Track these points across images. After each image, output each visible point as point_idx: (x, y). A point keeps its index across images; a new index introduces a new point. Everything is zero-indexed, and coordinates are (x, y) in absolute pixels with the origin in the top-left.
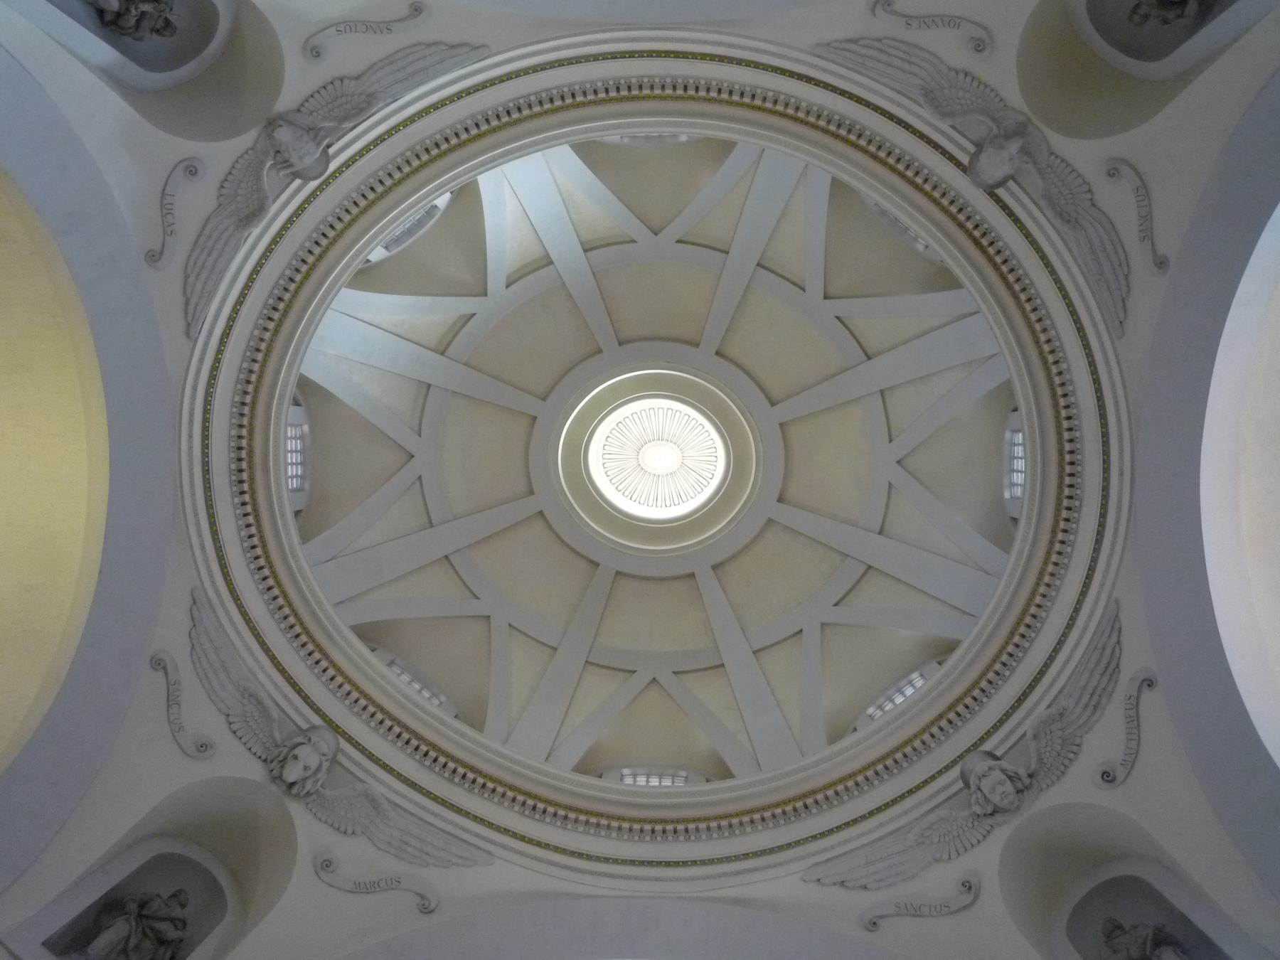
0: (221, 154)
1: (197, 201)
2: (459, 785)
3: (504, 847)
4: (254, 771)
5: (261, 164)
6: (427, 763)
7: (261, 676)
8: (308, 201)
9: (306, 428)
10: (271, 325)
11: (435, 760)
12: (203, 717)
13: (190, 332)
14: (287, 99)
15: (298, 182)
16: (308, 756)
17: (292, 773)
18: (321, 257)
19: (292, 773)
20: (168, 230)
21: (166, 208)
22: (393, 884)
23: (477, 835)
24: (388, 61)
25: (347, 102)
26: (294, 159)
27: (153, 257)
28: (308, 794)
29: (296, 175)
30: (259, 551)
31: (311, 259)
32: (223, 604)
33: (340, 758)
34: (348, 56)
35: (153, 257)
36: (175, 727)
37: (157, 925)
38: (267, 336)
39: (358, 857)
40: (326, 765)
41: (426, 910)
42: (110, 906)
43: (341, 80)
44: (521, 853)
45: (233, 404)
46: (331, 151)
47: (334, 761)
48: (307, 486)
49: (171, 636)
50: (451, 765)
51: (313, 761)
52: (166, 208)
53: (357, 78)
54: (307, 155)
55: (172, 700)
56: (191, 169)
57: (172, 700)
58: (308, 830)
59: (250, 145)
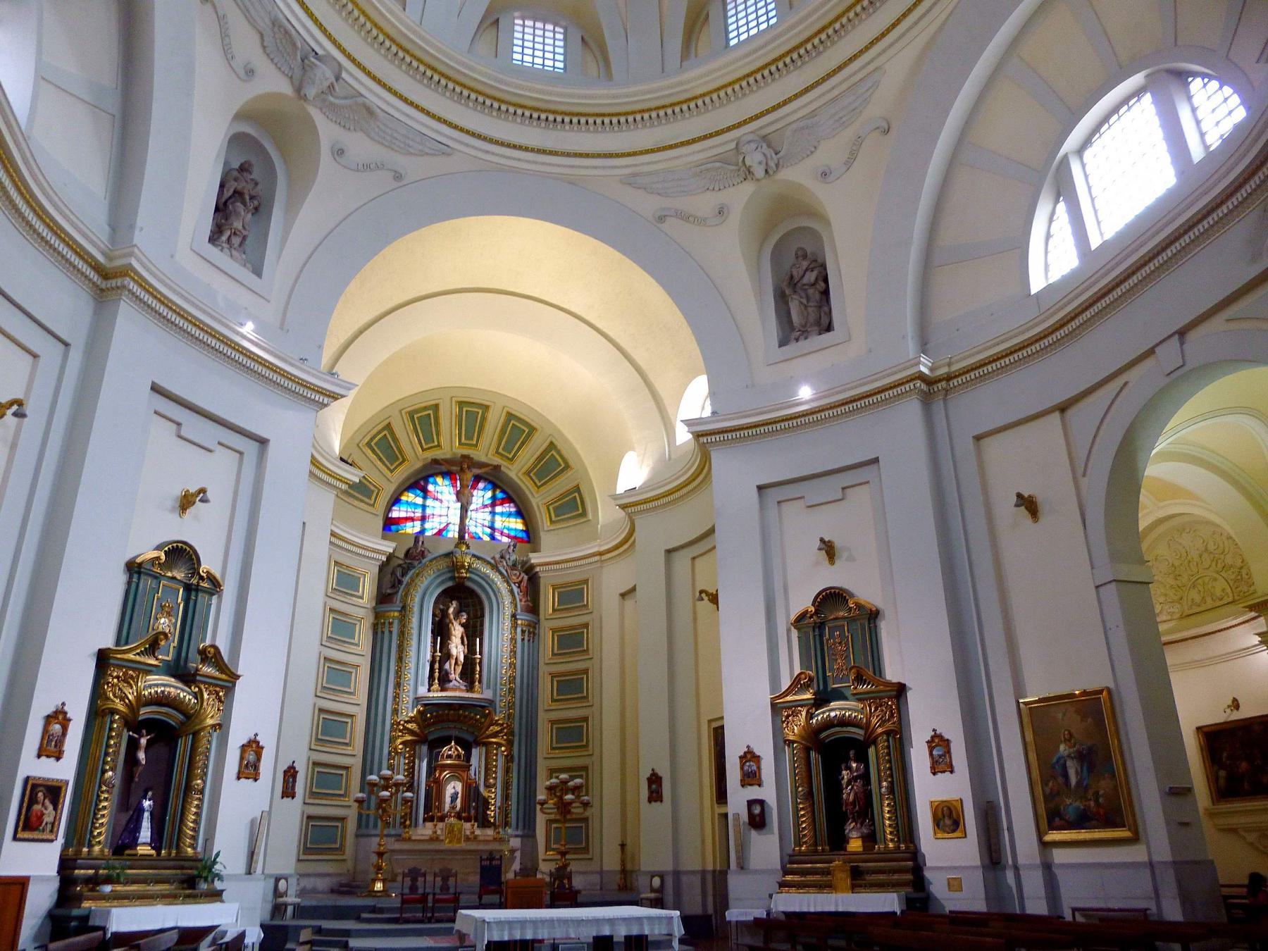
0: (327, 130)
1: (360, 146)
2: (825, 48)
3: (880, 54)
4: (748, 188)
5: (331, 103)
6: (799, 63)
7: (690, 159)
8: (353, 61)
9: (516, 14)
10: (443, 82)
11: (800, 57)
12: (704, 203)
13: (445, 150)
14: (286, 88)
15: (344, 75)
16: (754, 160)
17: (759, 172)
18: (392, 40)
19: (759, 172)
20: (380, 166)
21: (367, 167)
22: (859, 141)
23: (863, 67)
24: (246, 12)
25: (281, 41)
26: (326, 84)
27: (398, 177)
28: (777, 165)
29: (338, 78)
30: (607, 120)
31: (394, 49)
32: (636, 165)
33: (764, 132)
34: (247, 46)
35: (398, 177)
36: (702, 222)
37: (805, 281)
38: (451, 85)
39: (830, 152)
40: (765, 146)
41: (887, 131)
42: (781, 298)
43: (264, 47)
44: (891, 46)
45: (499, 117)
46: (320, 52)
47: (764, 138)
48: (564, 24)
49: (649, 204)
50: (809, 46)
51: (758, 157)
52: (367, 167)
53: (262, 36)
54: (324, 74)
55: (685, 217)
56: (339, 152)
57: (685, 217)
58: (798, 175)
59: (318, 111)
